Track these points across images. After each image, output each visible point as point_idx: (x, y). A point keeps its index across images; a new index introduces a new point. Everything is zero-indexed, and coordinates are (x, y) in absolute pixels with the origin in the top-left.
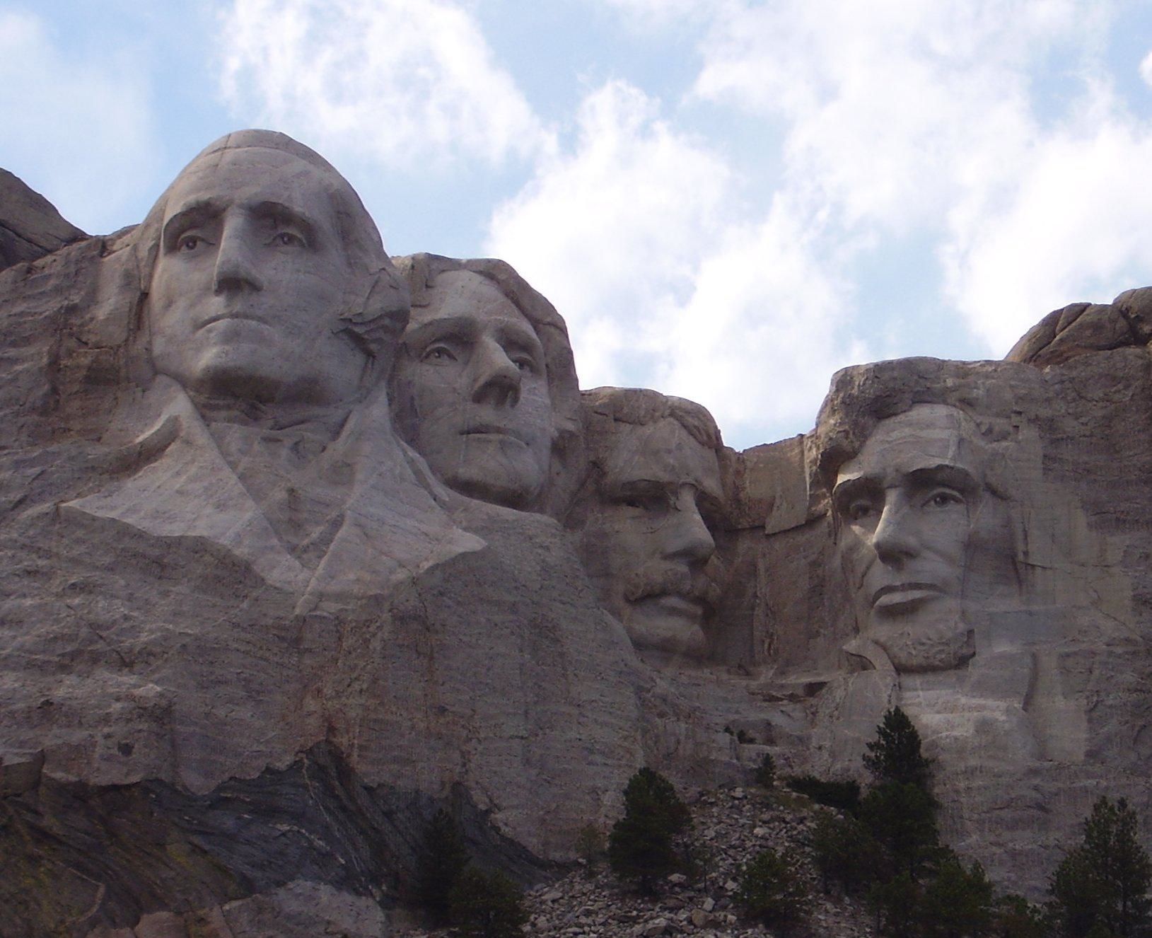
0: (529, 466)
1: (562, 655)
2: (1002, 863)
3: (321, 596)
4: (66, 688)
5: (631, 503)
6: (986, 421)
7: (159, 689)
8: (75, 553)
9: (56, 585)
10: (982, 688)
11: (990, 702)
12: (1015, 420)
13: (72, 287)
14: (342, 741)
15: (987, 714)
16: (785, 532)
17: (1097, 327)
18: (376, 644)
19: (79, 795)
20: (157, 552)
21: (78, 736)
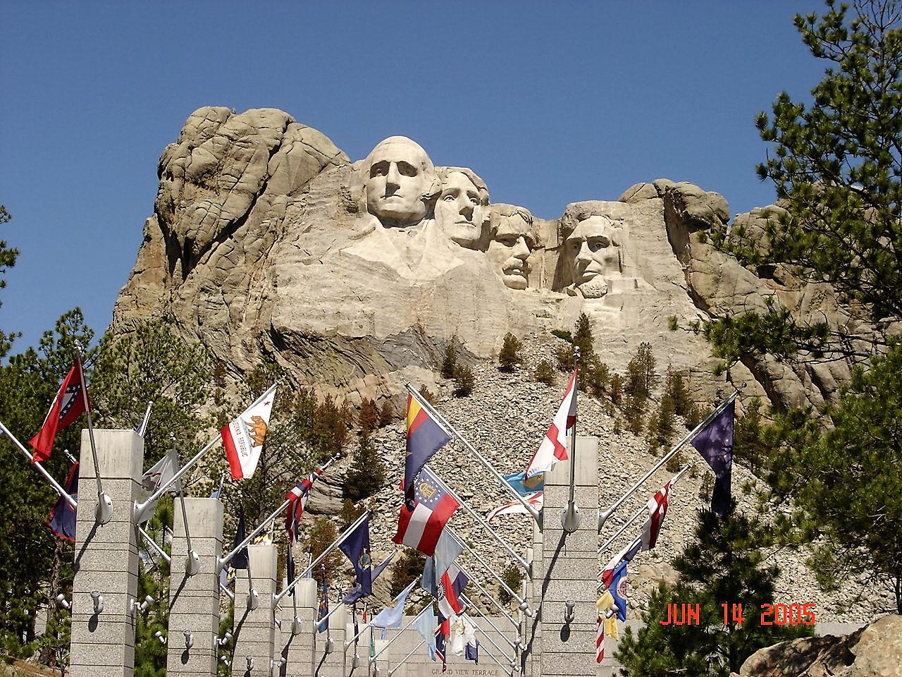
0: (475, 233)
1: (485, 295)
2: (613, 358)
3: (416, 280)
4: (344, 308)
5: (505, 240)
6: (613, 222)
7: (370, 309)
8: (345, 266)
9: (340, 274)
10: (608, 303)
11: (611, 308)
12: (622, 222)
13: (343, 180)
14: (421, 323)
15: (611, 314)
16: (551, 249)
17: (647, 192)
18: (432, 295)
19: (348, 339)
20: (369, 265)
21: (347, 322)
